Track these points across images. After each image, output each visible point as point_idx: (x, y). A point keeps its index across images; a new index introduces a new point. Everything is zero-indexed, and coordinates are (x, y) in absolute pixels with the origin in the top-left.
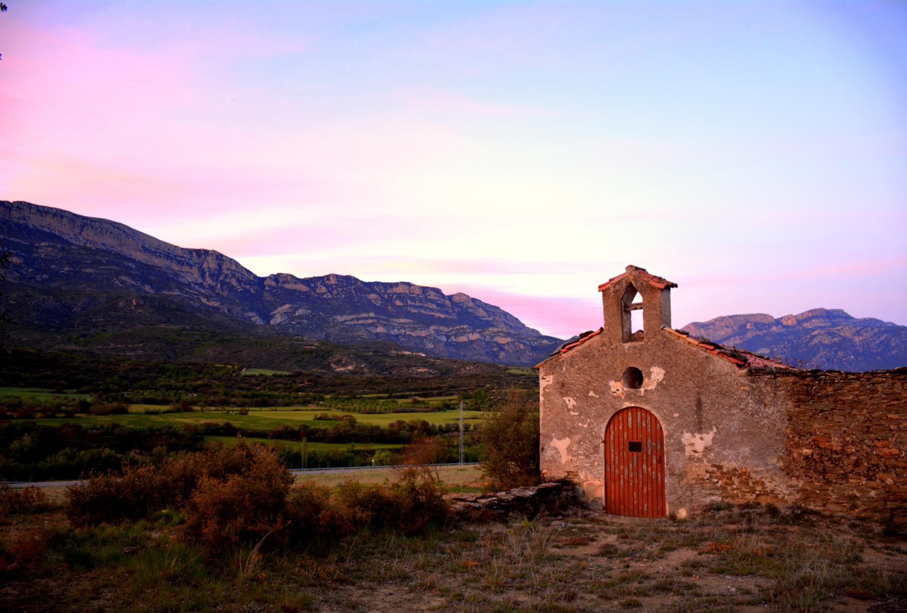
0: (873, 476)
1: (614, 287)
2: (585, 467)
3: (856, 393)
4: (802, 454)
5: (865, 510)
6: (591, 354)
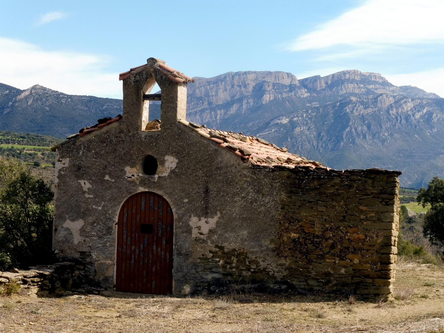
0: (344, 257)
1: (135, 77)
2: (98, 247)
3: (337, 187)
4: (290, 238)
5: (336, 285)
6: (109, 140)
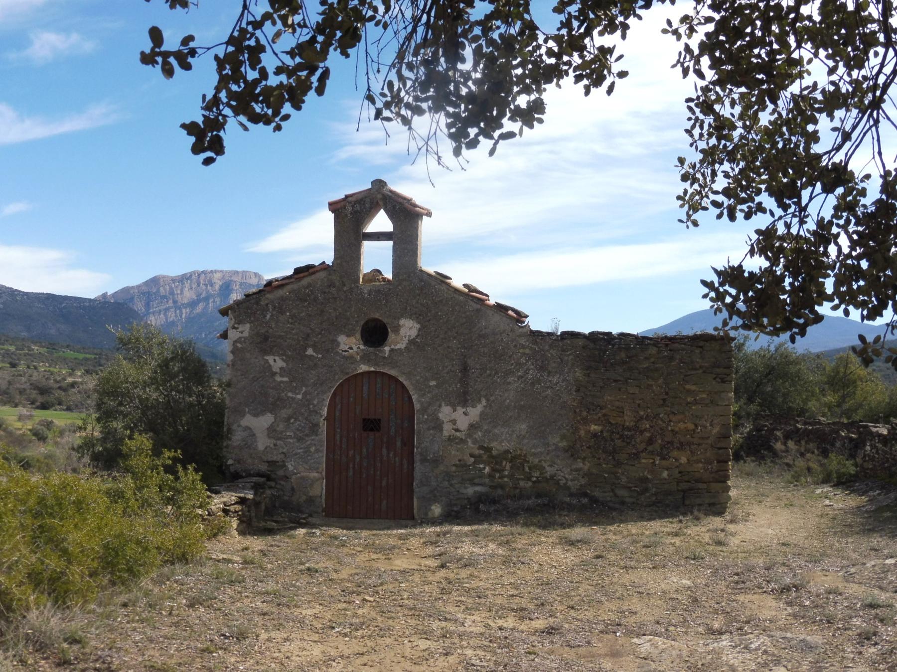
1: (353, 206)
2: (296, 454)
3: (652, 360)
4: (589, 431)
5: (655, 494)
6: (312, 297)
